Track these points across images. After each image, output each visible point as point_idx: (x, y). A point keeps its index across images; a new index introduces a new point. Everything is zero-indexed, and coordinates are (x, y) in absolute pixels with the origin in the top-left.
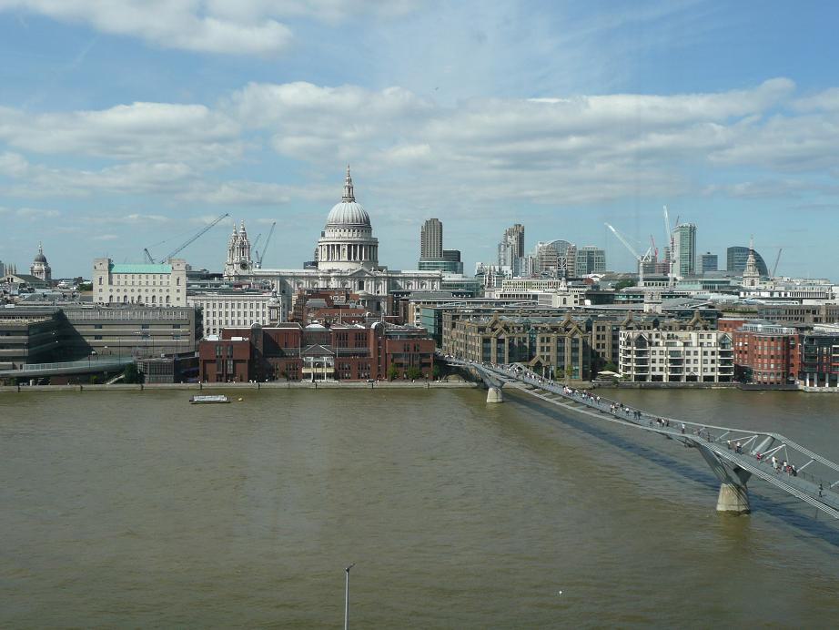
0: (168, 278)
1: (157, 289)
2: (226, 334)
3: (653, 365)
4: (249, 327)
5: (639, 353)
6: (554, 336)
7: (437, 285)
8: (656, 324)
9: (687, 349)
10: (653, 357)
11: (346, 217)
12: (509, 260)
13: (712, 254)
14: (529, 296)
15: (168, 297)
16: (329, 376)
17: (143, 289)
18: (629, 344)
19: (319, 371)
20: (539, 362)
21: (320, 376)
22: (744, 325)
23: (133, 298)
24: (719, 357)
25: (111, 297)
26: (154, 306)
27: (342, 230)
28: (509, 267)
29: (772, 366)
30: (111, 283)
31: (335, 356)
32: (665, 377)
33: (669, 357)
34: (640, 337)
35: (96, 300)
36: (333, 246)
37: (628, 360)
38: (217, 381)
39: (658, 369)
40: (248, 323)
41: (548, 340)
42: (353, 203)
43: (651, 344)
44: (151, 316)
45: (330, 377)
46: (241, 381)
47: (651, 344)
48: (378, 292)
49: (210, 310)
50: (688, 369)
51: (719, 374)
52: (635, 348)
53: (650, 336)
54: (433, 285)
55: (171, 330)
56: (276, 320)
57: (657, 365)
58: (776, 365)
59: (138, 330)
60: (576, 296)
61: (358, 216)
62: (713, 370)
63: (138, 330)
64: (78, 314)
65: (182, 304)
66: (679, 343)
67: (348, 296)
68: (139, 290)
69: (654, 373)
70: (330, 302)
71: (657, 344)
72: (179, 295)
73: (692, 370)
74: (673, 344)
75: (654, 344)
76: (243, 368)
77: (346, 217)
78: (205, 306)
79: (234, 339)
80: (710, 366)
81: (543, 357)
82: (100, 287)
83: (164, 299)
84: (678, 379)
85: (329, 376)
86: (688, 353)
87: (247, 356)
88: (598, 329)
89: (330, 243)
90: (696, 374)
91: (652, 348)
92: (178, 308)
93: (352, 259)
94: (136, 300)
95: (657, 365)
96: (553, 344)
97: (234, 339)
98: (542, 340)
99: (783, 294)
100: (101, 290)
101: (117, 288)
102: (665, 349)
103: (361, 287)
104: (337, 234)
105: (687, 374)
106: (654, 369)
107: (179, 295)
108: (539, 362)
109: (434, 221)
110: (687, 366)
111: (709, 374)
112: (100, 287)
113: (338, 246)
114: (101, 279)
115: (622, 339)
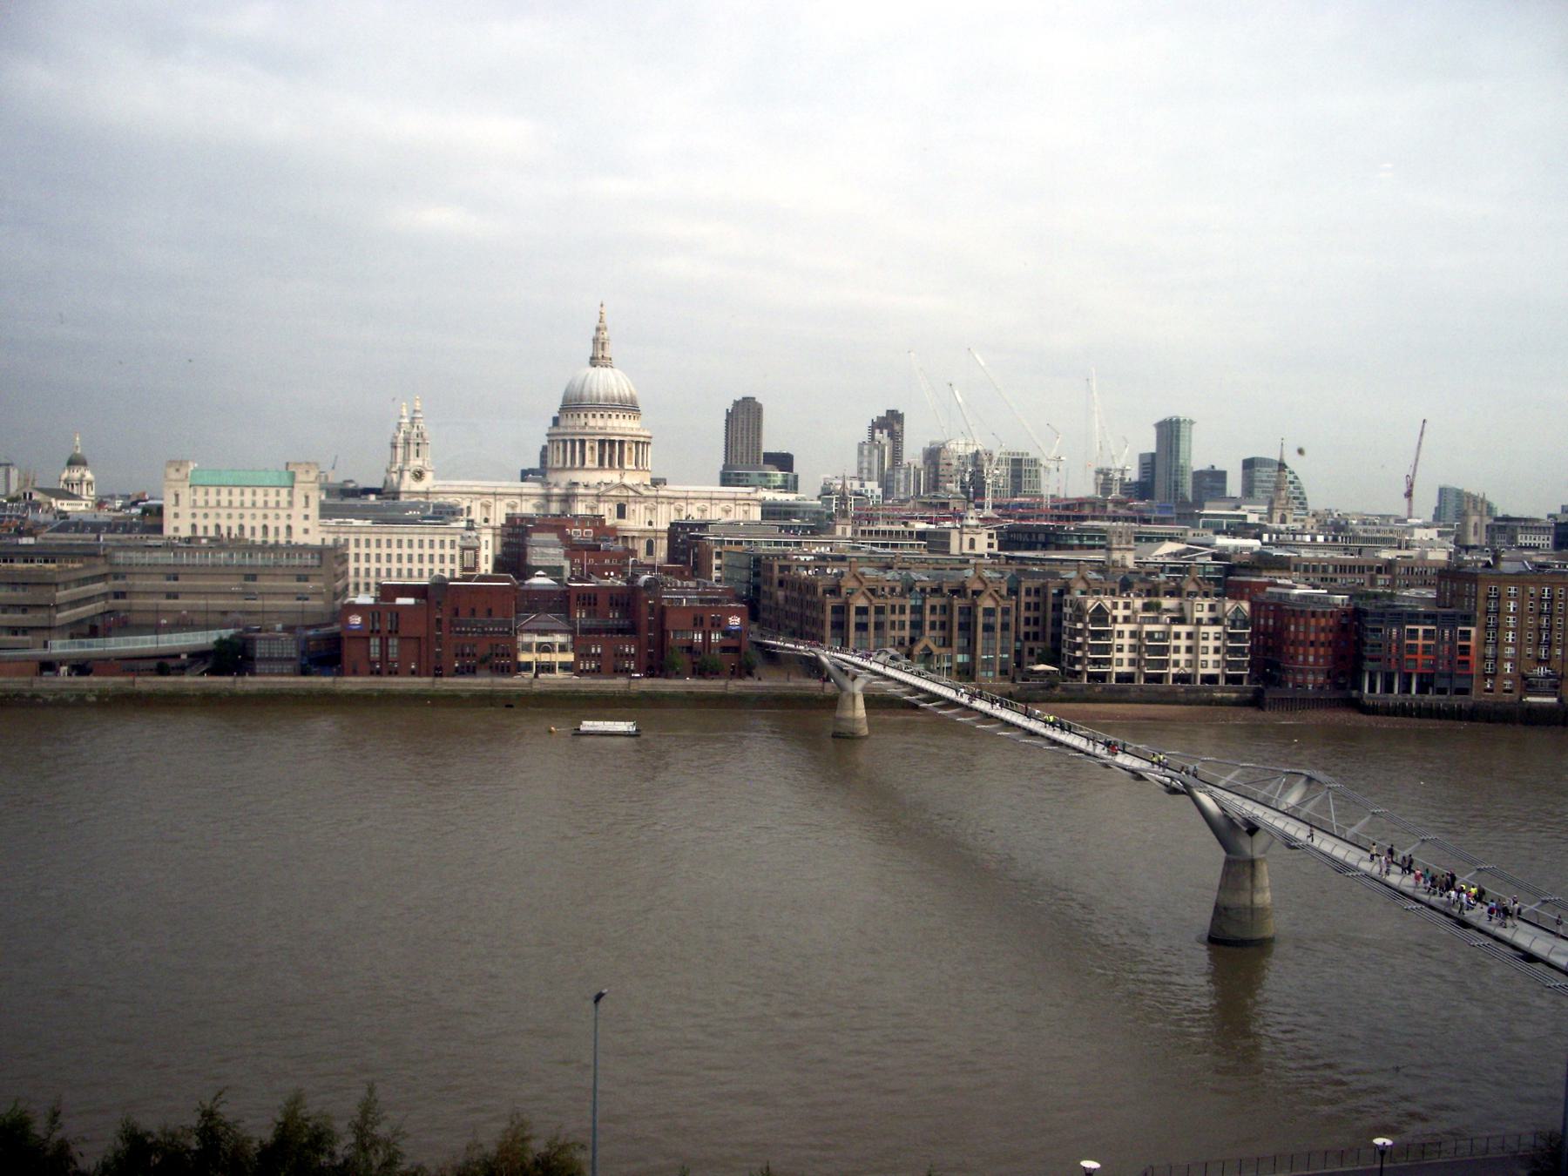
0: (290, 494)
1: (271, 513)
2: (388, 592)
3: (1118, 655)
4: (425, 581)
5: (1096, 635)
6: (958, 602)
7: (756, 514)
8: (1126, 586)
9: (1176, 628)
11: (595, 391)
13: (1217, 468)
14: (911, 533)
15: (289, 528)
16: (565, 667)
17: (247, 513)
19: (545, 657)
20: (927, 647)
21: (549, 668)
22: (1269, 589)
23: (229, 529)
25: (194, 527)
26: (265, 542)
29: (1311, 659)
31: (572, 632)
34: (1100, 609)
35: (168, 531)
37: (1079, 647)
38: (372, 673)
40: (426, 574)
43: (1115, 619)
44: (259, 559)
48: (650, 523)
49: (363, 550)
50: (1176, 664)
53: (1115, 606)
54: (746, 512)
55: (294, 585)
56: (473, 569)
58: (1316, 657)
59: (235, 584)
60: (990, 536)
63: (235, 584)
64: (139, 555)
65: (314, 539)
66: (1165, 618)
67: (595, 529)
68: (242, 516)
69: (1119, 669)
71: (1126, 620)
72: (307, 524)
73: (1182, 664)
74: (1156, 621)
75: (1120, 619)
79: (400, 601)
83: (283, 531)
84: (1158, 679)
86: (1177, 636)
88: (1028, 592)
89: (567, 438)
90: (1189, 670)
91: (1118, 627)
92: (305, 548)
93: (607, 466)
94: (235, 531)
97: (400, 601)
98: (933, 609)
99: (1330, 538)
100: (176, 515)
101: (204, 511)
103: (621, 512)
105: (1174, 670)
107: (307, 524)
108: (927, 647)
110: (1174, 657)
111: (1210, 670)
113: (583, 442)
114: (177, 496)
115: (1067, 610)
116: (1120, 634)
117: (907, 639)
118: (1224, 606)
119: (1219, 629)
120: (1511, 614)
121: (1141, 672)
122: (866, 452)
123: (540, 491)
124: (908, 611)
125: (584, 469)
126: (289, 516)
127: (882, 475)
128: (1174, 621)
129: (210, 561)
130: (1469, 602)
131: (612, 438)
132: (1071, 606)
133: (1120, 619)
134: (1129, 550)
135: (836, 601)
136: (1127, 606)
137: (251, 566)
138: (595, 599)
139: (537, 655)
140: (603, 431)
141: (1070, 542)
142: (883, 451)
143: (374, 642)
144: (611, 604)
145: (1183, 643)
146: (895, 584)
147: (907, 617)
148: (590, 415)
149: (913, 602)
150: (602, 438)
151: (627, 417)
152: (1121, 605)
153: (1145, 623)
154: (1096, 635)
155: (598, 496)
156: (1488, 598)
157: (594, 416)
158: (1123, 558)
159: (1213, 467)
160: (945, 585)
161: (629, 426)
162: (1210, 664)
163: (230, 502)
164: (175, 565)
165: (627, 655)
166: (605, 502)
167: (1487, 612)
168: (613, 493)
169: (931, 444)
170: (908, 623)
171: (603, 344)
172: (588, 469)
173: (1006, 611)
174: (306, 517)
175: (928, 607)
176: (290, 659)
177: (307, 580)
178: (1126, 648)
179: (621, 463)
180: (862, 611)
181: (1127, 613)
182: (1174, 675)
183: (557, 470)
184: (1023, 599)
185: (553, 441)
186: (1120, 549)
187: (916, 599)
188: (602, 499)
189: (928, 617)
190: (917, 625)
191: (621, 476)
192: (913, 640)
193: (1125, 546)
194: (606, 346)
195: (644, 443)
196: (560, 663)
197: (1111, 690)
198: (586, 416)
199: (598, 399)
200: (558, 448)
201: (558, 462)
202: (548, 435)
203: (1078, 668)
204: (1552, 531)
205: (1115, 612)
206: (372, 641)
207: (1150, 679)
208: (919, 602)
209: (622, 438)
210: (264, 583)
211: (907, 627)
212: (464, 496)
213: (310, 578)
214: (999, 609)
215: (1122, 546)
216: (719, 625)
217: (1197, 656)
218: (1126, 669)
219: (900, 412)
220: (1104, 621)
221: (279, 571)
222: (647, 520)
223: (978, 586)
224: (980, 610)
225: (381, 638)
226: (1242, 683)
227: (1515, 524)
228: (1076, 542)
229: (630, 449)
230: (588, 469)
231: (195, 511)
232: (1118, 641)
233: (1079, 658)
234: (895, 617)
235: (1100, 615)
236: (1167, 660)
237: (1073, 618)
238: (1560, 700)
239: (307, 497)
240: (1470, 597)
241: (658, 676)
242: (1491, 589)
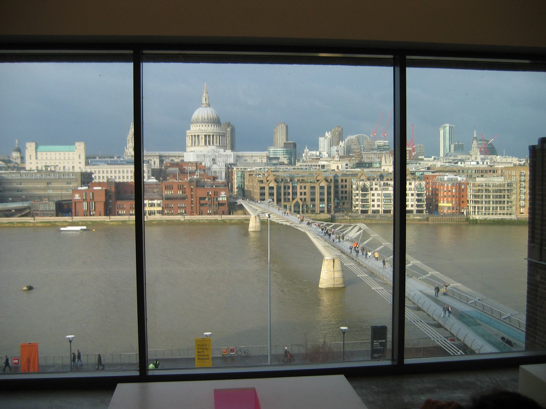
0: (73, 154)
3: (373, 203)
4: (105, 181)
12: (326, 150)
15: (73, 167)
16: (159, 212)
18: (357, 189)
20: (297, 202)
24: (416, 197)
27: (201, 126)
28: (326, 153)
30: (36, 158)
33: (383, 197)
34: (365, 186)
36: (195, 136)
38: (84, 216)
39: (376, 206)
40: (105, 178)
41: (305, 188)
42: (208, 108)
43: (372, 189)
44: (52, 176)
45: (159, 213)
46: (100, 215)
47: (372, 189)
51: (416, 208)
52: (361, 192)
55: (65, 185)
57: (376, 203)
62: (412, 206)
63: (43, 185)
67: (197, 167)
69: (372, 208)
71: (376, 189)
74: (387, 189)
75: (374, 189)
76: (101, 207)
77: (203, 118)
78: (97, 172)
81: (301, 199)
82: (30, 161)
85: (159, 212)
87: (103, 199)
89: (193, 134)
91: (372, 192)
95: (376, 203)
96: (307, 190)
98: (301, 188)
100: (31, 163)
102: (380, 192)
104: (198, 128)
106: (373, 206)
108: (297, 202)
112: (30, 161)
113: (198, 136)
114: (30, 156)
115: (354, 186)
117: (291, 199)
124: (291, 188)
126: (73, 163)
129: (34, 177)
131: (210, 134)
132: (355, 185)
134: (390, 166)
135: (262, 185)
137: (50, 179)
138: (172, 186)
139: (149, 208)
140: (206, 131)
143: (85, 204)
144: (178, 189)
148: (201, 126)
150: (205, 134)
153: (383, 190)
156: (520, 176)
157: (203, 126)
158: (388, 169)
163: (46, 158)
164: (20, 179)
165: (183, 207)
167: (520, 181)
170: (291, 193)
173: (329, 188)
174: (80, 163)
176: (54, 211)
177: (70, 184)
183: (189, 147)
186: (387, 165)
189: (299, 191)
192: (293, 199)
193: (389, 164)
196: (157, 211)
197: (369, 216)
198: (200, 126)
200: (190, 138)
203: (357, 208)
206: (84, 203)
209: (213, 134)
210: (53, 185)
212: (153, 157)
213: (72, 183)
215: (387, 164)
216: (217, 195)
220: (367, 190)
221: (60, 181)
225: (87, 202)
226: (423, 213)
229: (216, 138)
230: (201, 146)
231: (38, 161)
232: (373, 198)
233: (358, 204)
234: (287, 191)
239: (80, 156)
241: (195, 215)
242: (521, 172)
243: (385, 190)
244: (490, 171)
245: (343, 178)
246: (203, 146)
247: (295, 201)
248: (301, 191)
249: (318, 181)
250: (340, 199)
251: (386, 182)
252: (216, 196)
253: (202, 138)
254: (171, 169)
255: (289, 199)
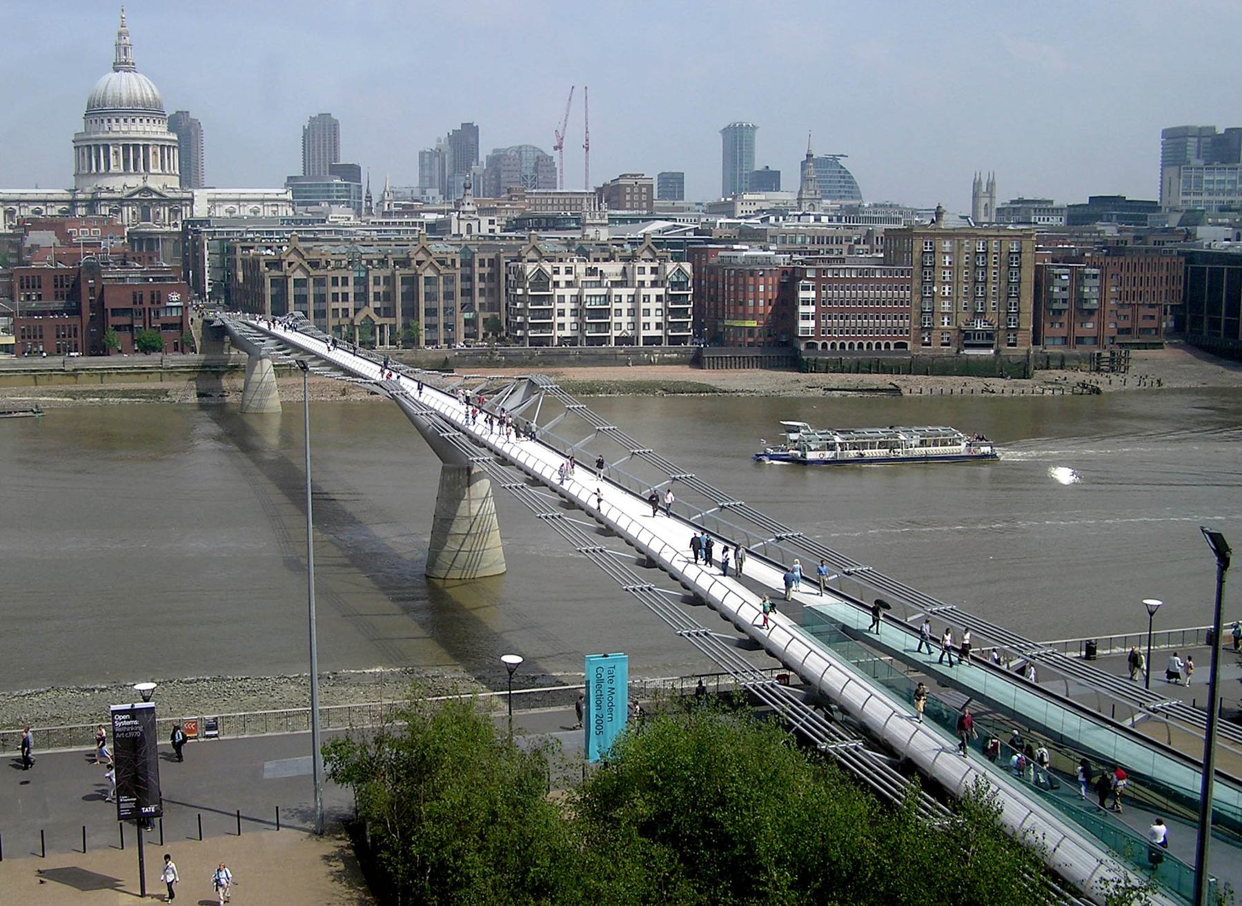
3: (560, 320)
5: (538, 300)
9: (616, 291)
10: (559, 306)
12: (437, 184)
22: (720, 253)
32: (579, 339)
34: (540, 272)
37: (520, 312)
43: (556, 284)
47: (556, 284)
61: (138, 95)
70: (65, 237)
71: (569, 284)
73: (624, 327)
74: (599, 284)
75: (562, 284)
80: (654, 319)
88: (482, 265)
91: (558, 292)
93: (132, 170)
105: (617, 333)
106: (562, 326)
109: (325, 117)
110: (616, 320)
113: (107, 147)
116: (562, 298)
118: (665, 268)
119: (661, 291)
120: (947, 268)
121: (584, 335)
122: (427, 161)
123: (70, 197)
124: (351, 283)
125: (109, 174)
127: (443, 183)
128: (616, 284)
130: (908, 256)
133: (562, 284)
136: (568, 272)
138: (39, 280)
141: (568, 225)
142: (444, 159)
145: (625, 305)
146: (340, 257)
147: (350, 289)
148: (114, 121)
149: (356, 275)
151: (151, 121)
152: (562, 271)
153: (587, 287)
154: (538, 300)
155: (121, 199)
157: (117, 121)
159: (767, 167)
160: (389, 256)
161: (154, 129)
162: (653, 321)
166: (128, 205)
168: (137, 196)
169: (495, 151)
171: (125, 49)
172: (115, 174)
173: (449, 280)
175: (371, 278)
178: (568, 313)
179: (146, 167)
180: (297, 282)
181: (570, 278)
182: (615, 337)
184: (476, 270)
185: (78, 147)
187: (359, 271)
188: (126, 203)
189: (372, 289)
190: (362, 297)
191: (145, 180)
192: (356, 311)
193: (599, 221)
194: (129, 51)
195: (169, 146)
199: (121, 103)
200: (83, 154)
201: (83, 168)
202: (73, 142)
204: (1065, 213)
205: (556, 278)
207: (592, 341)
208: (363, 274)
211: (351, 298)
214: (441, 278)
215: (595, 222)
216: (159, 302)
217: (639, 319)
218: (567, 333)
219: (475, 125)
222: (172, 223)
223: (421, 257)
224: (422, 280)
227: (1030, 206)
228: (574, 225)
229: (155, 153)
232: (559, 306)
234: (338, 289)
235: (541, 280)
236: (609, 323)
237: (516, 285)
238: (997, 352)
240: (908, 252)
243: (591, 287)
244: (849, 239)
245: (483, 256)
246: (121, 174)
247: (362, 315)
248: (377, 289)
249: (419, 263)
250: (477, 309)
251: (595, 265)
252: (156, 306)
253: (116, 153)
254: (34, 237)
255: (346, 310)
